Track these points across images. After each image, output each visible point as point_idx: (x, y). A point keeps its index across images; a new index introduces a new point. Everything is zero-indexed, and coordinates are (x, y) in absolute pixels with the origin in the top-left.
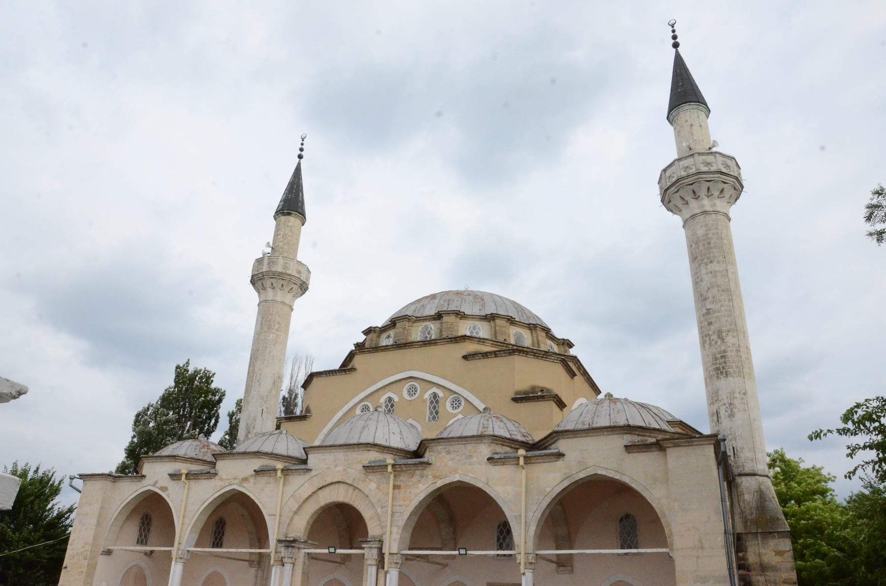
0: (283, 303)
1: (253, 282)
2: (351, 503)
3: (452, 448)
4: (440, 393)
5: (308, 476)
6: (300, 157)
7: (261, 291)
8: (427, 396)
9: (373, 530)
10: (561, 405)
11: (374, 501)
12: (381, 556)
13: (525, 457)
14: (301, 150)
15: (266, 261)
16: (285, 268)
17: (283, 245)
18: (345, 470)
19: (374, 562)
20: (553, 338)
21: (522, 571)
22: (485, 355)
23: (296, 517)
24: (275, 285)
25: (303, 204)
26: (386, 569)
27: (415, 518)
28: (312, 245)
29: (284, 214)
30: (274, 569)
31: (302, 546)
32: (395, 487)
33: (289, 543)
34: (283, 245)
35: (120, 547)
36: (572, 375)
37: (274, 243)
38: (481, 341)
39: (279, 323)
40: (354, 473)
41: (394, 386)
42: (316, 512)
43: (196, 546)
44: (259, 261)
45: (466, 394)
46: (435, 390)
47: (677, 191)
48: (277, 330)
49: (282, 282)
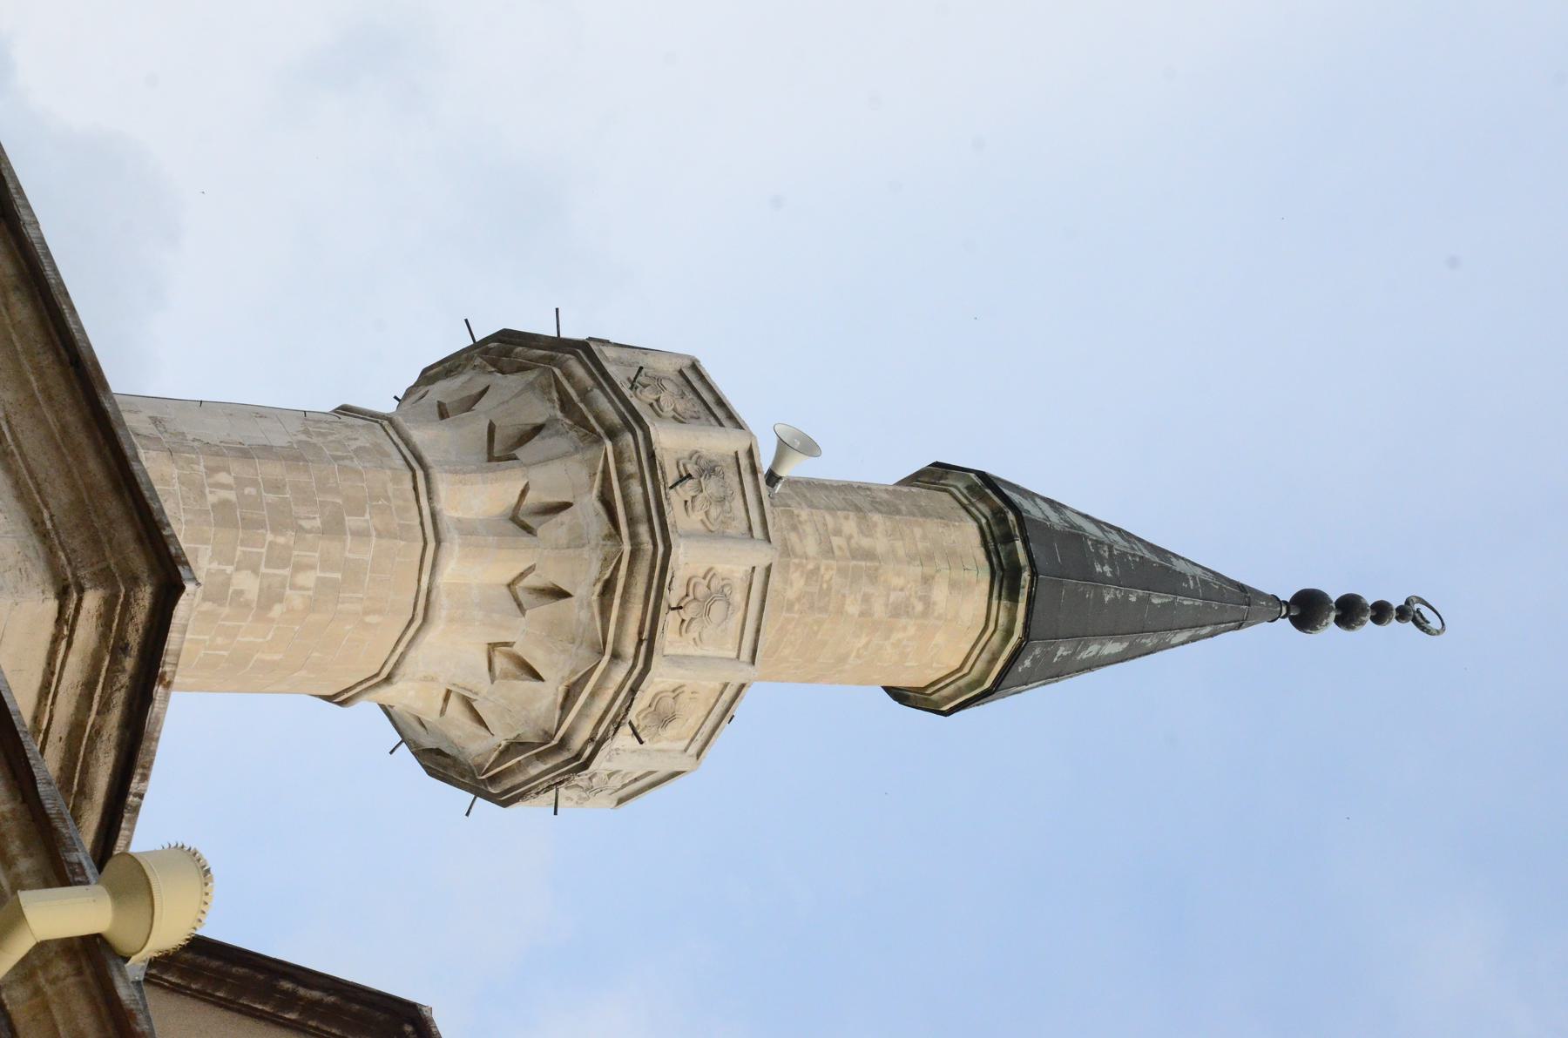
0: (423, 611)
6: (1307, 610)
14: (1350, 611)
15: (717, 443)
16: (710, 594)
24: (554, 529)
37: (810, 488)
39: (270, 597)
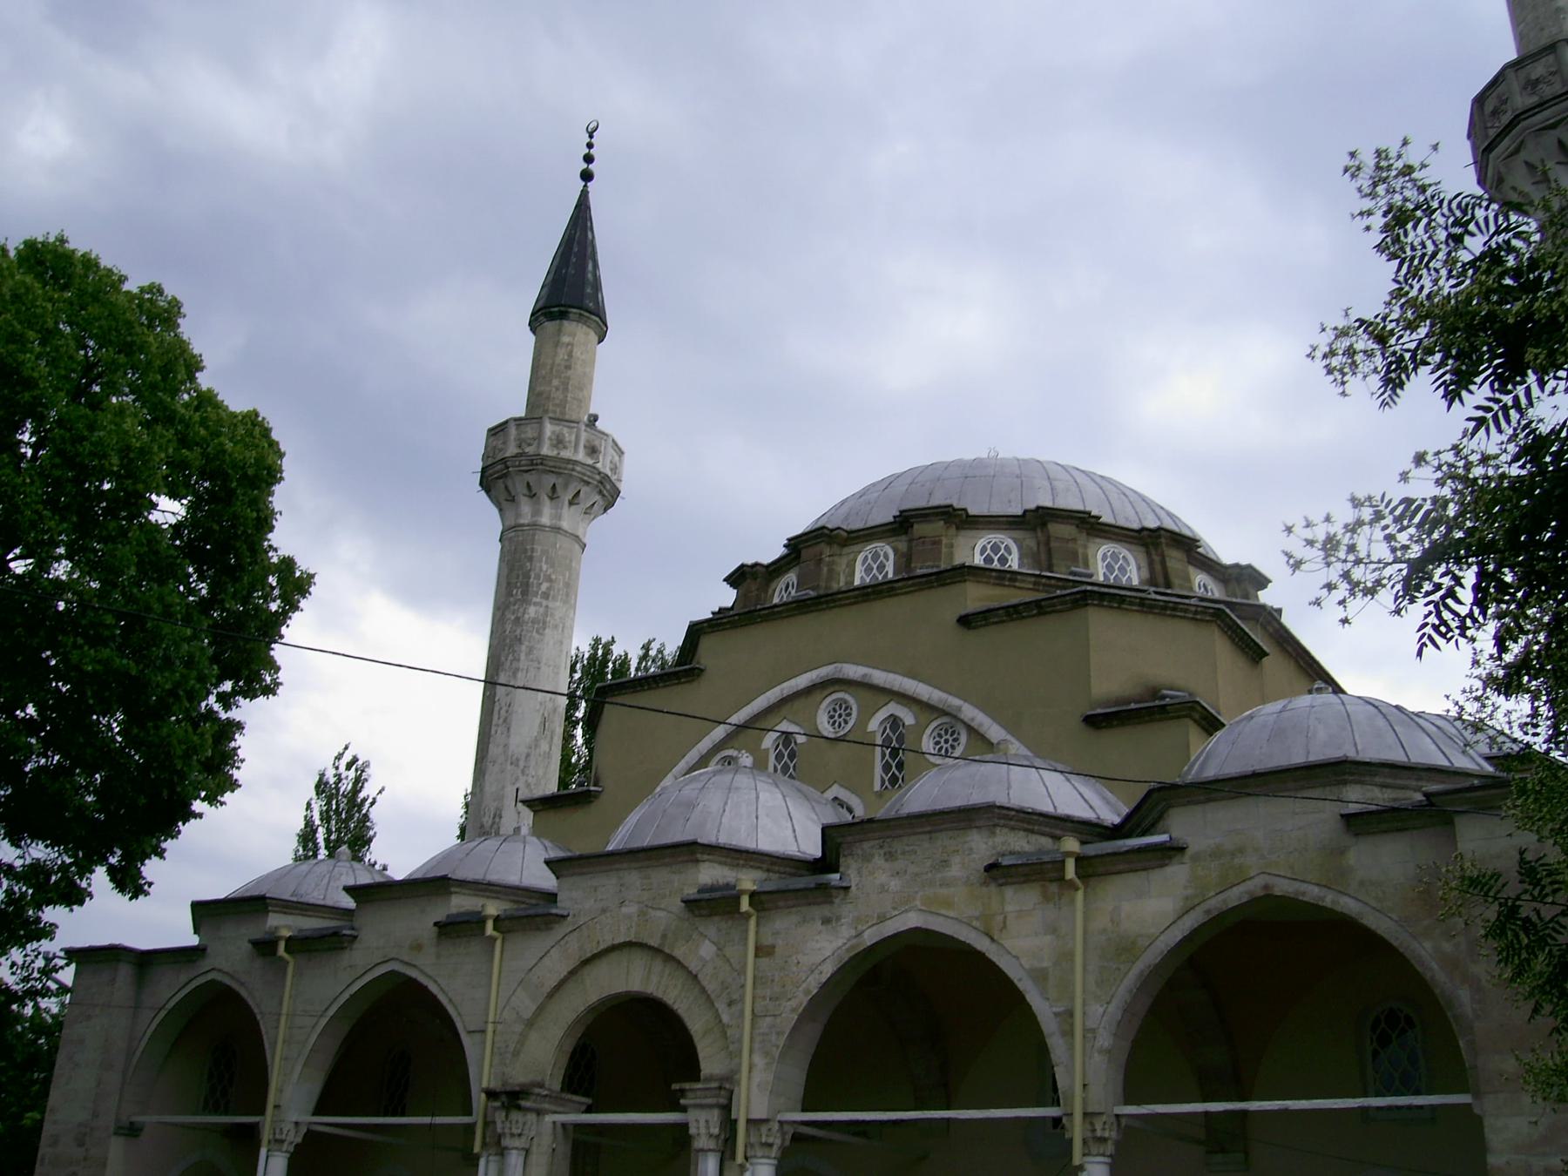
1: (487, 482)
2: (659, 994)
3: (898, 846)
4: (908, 718)
5: (561, 930)
6: (587, 176)
7: (505, 504)
8: (874, 725)
9: (711, 1062)
10: (1211, 724)
11: (711, 986)
12: (729, 1125)
13: (1080, 860)
14: (589, 159)
17: (553, 388)
18: (642, 914)
19: (712, 1144)
20: (1209, 565)
21: (1077, 1161)
22: (1013, 613)
23: (534, 1036)
25: (597, 286)
26: (740, 1158)
27: (814, 1031)
28: (627, 385)
29: (551, 317)
30: (482, 1162)
31: (546, 1106)
32: (761, 951)
33: (511, 1098)
34: (553, 388)
35: (155, 1118)
36: (1255, 654)
38: (1005, 577)
39: (549, 579)
40: (665, 916)
41: (799, 704)
42: (577, 1021)
43: (318, 1111)
44: (497, 431)
45: (969, 712)
46: (893, 708)
47: (1517, 151)
48: (546, 596)
49: (550, 480)
